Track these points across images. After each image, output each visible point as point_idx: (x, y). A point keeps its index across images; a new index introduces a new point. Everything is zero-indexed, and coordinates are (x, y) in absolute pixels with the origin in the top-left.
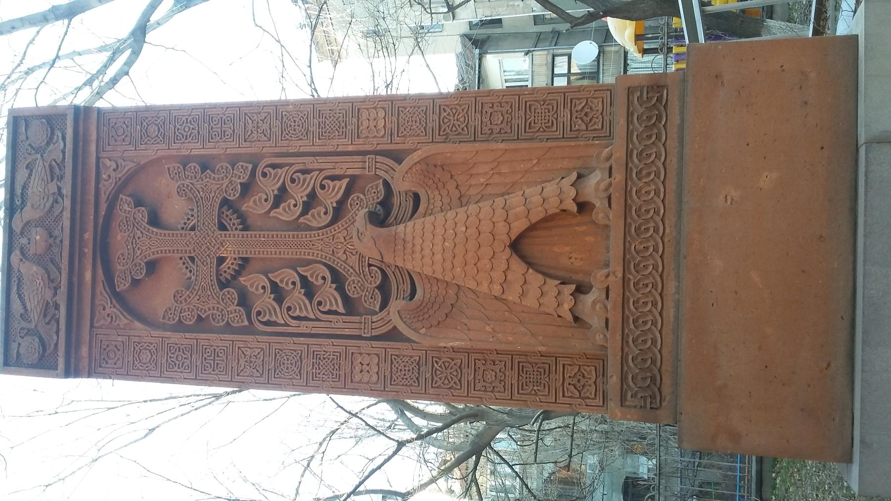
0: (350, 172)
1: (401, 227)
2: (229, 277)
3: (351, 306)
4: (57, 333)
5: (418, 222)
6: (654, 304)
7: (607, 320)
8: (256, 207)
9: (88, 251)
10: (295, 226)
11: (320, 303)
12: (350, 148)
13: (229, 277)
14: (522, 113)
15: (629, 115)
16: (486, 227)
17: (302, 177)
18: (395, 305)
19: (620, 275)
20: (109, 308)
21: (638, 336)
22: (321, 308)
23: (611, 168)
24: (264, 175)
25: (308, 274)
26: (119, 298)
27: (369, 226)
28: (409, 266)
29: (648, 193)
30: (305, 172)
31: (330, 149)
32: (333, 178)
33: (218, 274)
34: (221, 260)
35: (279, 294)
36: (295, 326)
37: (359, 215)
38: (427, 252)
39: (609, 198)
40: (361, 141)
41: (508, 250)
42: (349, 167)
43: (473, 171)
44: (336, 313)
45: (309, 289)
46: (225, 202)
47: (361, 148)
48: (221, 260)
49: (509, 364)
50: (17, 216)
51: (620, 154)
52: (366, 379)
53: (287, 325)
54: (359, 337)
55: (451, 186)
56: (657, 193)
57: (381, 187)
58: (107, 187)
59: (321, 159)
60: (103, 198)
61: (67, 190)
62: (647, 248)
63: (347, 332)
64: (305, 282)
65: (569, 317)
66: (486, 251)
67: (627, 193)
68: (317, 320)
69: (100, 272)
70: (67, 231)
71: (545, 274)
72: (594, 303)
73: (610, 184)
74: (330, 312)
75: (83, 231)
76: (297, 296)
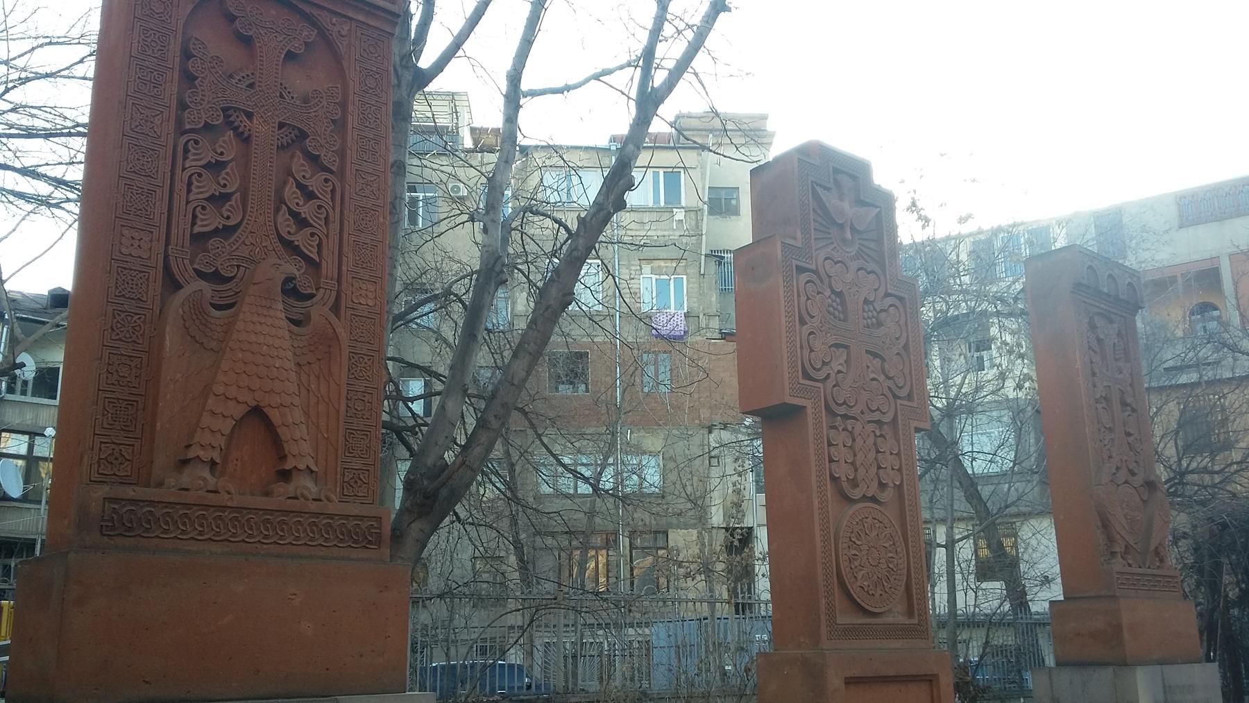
0: (324, 264)
1: (280, 306)
2: (232, 119)
3: (199, 239)
5: (284, 323)
6: (201, 533)
7: (187, 490)
8: (299, 165)
10: (281, 201)
11: (204, 208)
12: (344, 268)
13: (232, 119)
14: (362, 428)
17: (323, 216)
18: (206, 287)
19: (229, 504)
21: (172, 518)
22: (199, 209)
23: (320, 500)
24: (326, 180)
25: (233, 203)
27: (284, 276)
29: (298, 531)
31: (345, 249)
32: (319, 245)
34: (250, 116)
35: (216, 167)
37: (292, 267)
39: (296, 498)
40: (350, 280)
41: (254, 404)
42: (329, 267)
43: (322, 379)
44: (193, 224)
45: (219, 200)
46: (303, 135)
47: (344, 279)
48: (250, 116)
49: (135, 391)
51: (331, 509)
52: (124, 240)
53: (184, 169)
54: (167, 243)
56: (297, 538)
57: (309, 291)
60: (315, 12)
62: (251, 529)
63: (174, 231)
64: (226, 197)
65: (191, 454)
68: (188, 202)
71: (231, 437)
72: (204, 479)
73: (307, 499)
74: (194, 217)
76: (207, 187)
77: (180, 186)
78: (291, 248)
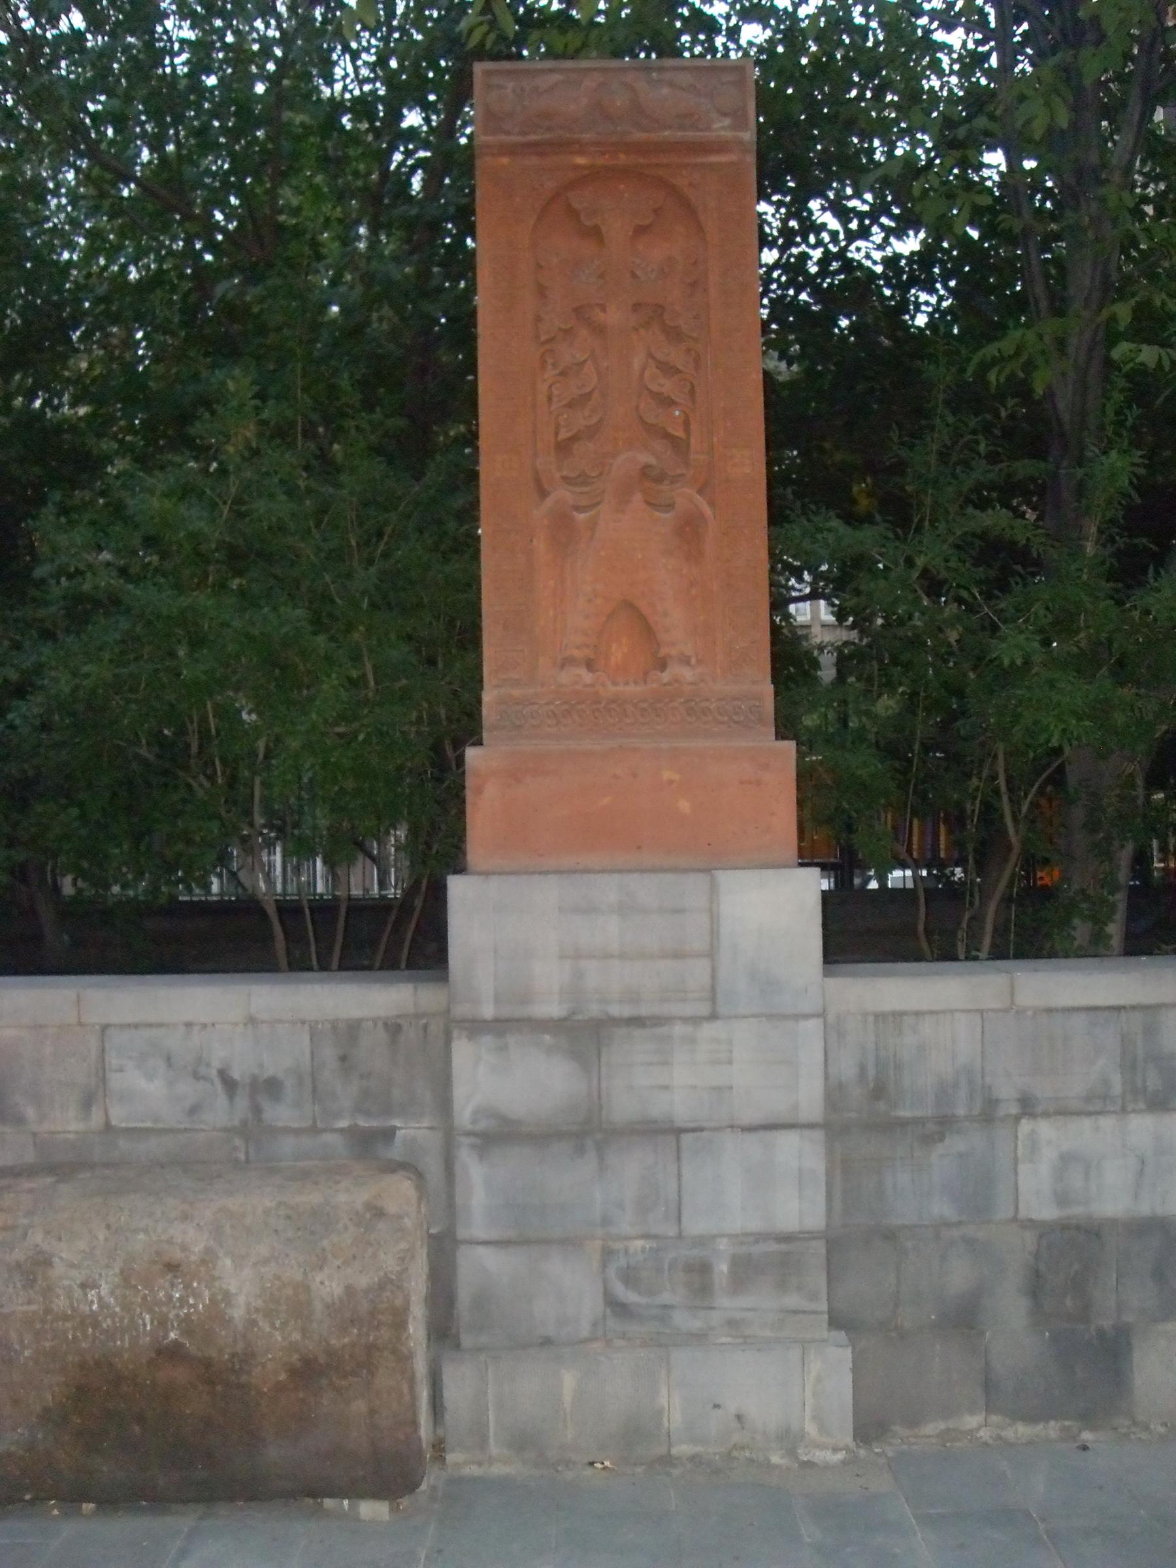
34: (604, 309)
48: (604, 309)
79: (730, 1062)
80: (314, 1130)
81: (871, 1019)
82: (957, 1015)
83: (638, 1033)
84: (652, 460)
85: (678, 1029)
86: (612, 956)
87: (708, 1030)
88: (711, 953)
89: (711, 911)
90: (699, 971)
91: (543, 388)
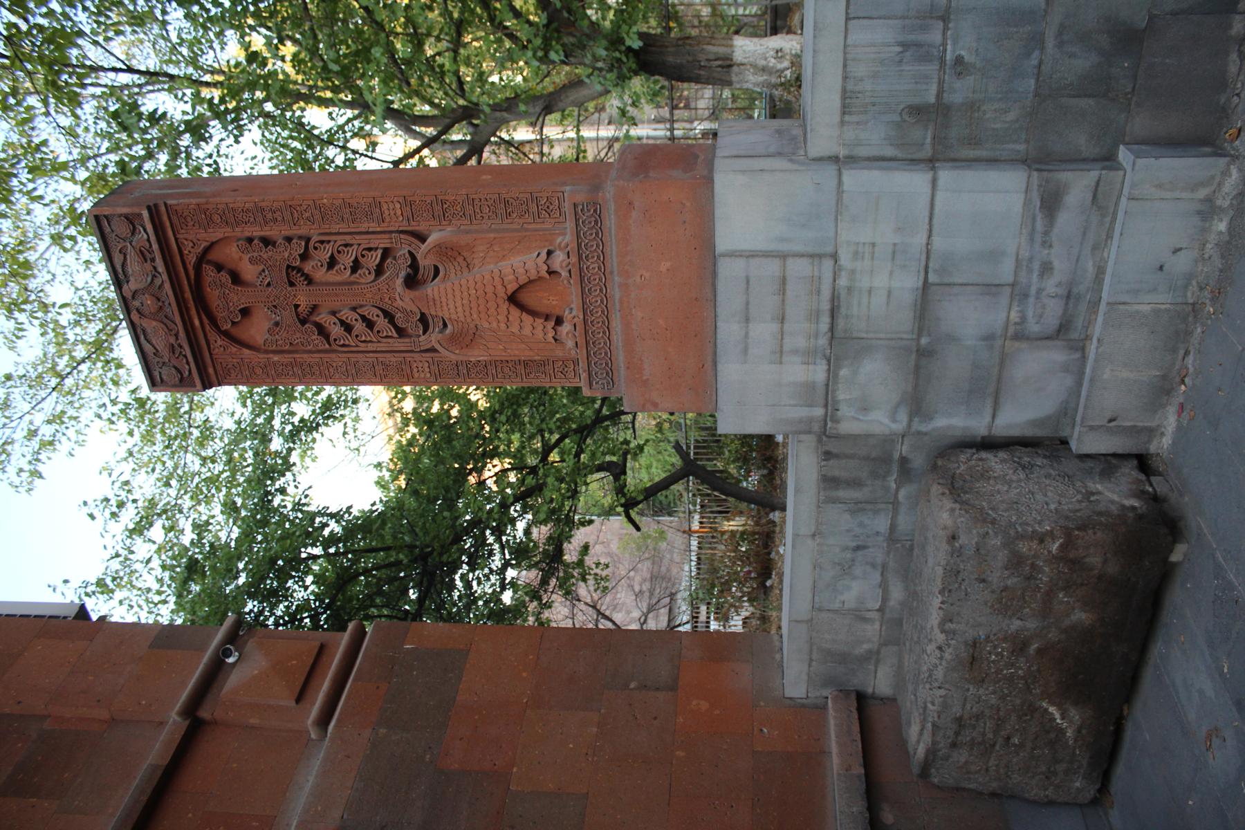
4: (188, 363)
9: (191, 304)
15: (577, 220)
16: (489, 289)
20: (218, 342)
26: (226, 334)
28: (440, 314)
30: (346, 245)
32: (370, 249)
33: (298, 315)
34: (297, 306)
36: (363, 347)
38: (451, 306)
44: (391, 337)
45: (370, 324)
48: (297, 306)
50: (125, 287)
55: (460, 259)
58: (192, 260)
59: (357, 237)
60: (190, 268)
61: (161, 268)
66: (492, 304)
67: (581, 269)
69: (204, 317)
70: (170, 293)
74: (387, 337)
75: (182, 292)
77: (370, 347)
78: (379, 271)
79: (873, 245)
80: (895, 504)
81: (847, 118)
82: (849, 41)
83: (843, 311)
84: (403, 274)
85: (843, 282)
86: (782, 328)
87: (845, 258)
88: (783, 256)
89: (748, 257)
90: (798, 268)
91: (363, 347)
